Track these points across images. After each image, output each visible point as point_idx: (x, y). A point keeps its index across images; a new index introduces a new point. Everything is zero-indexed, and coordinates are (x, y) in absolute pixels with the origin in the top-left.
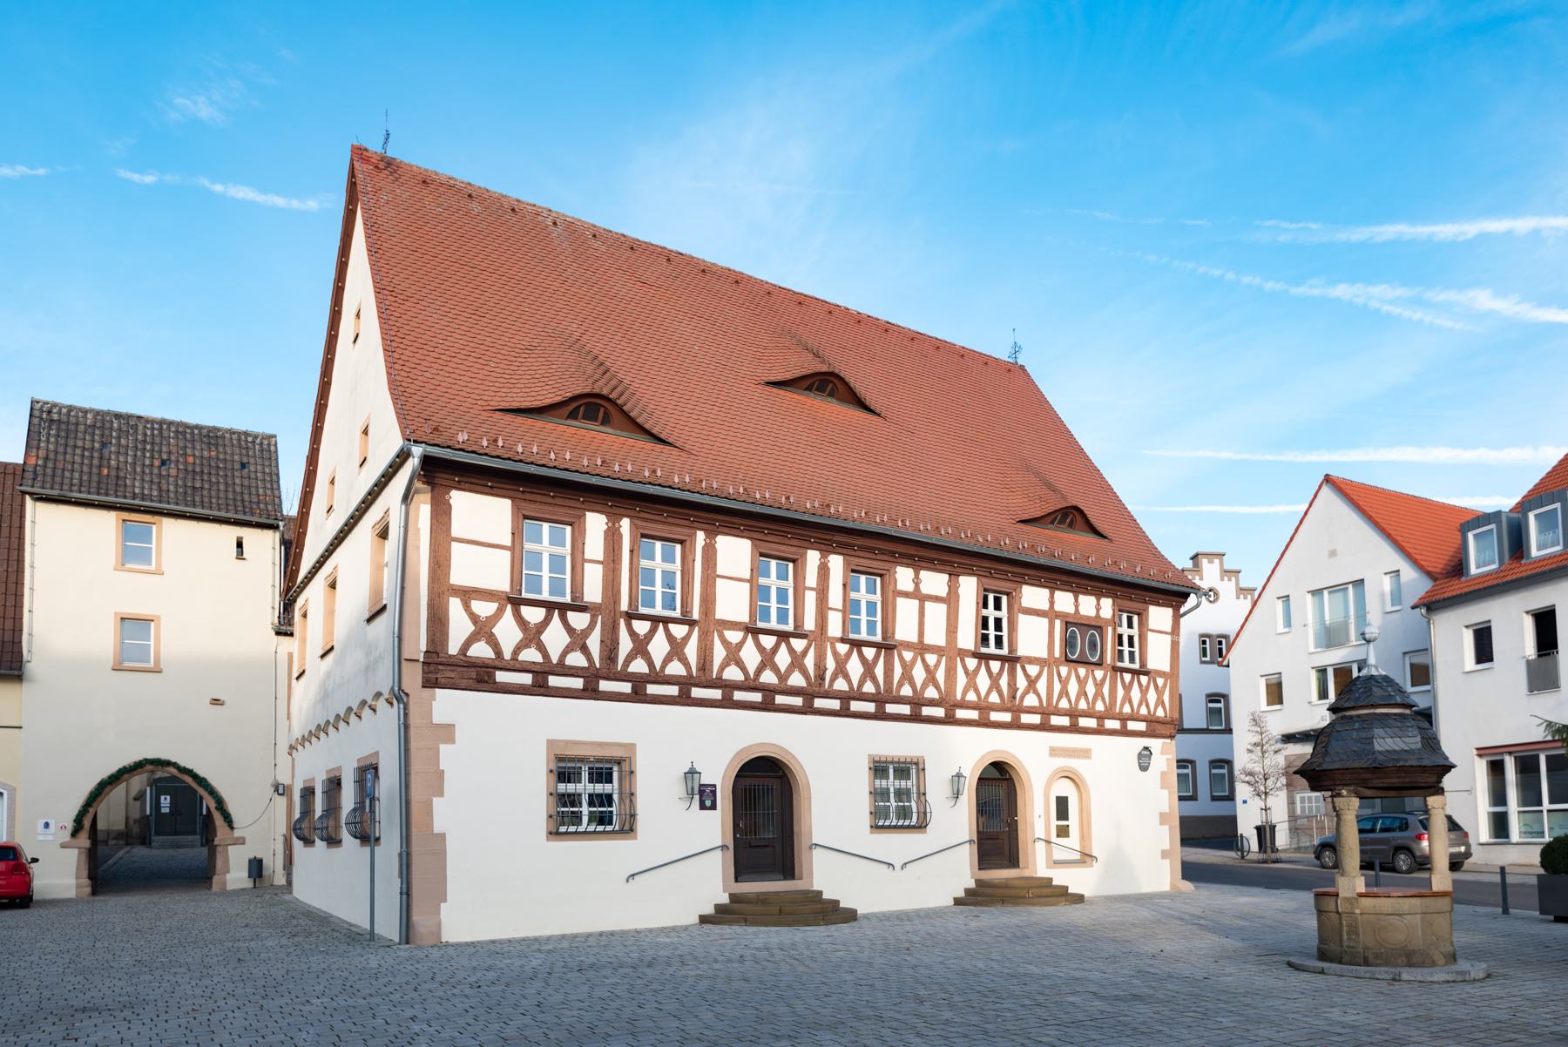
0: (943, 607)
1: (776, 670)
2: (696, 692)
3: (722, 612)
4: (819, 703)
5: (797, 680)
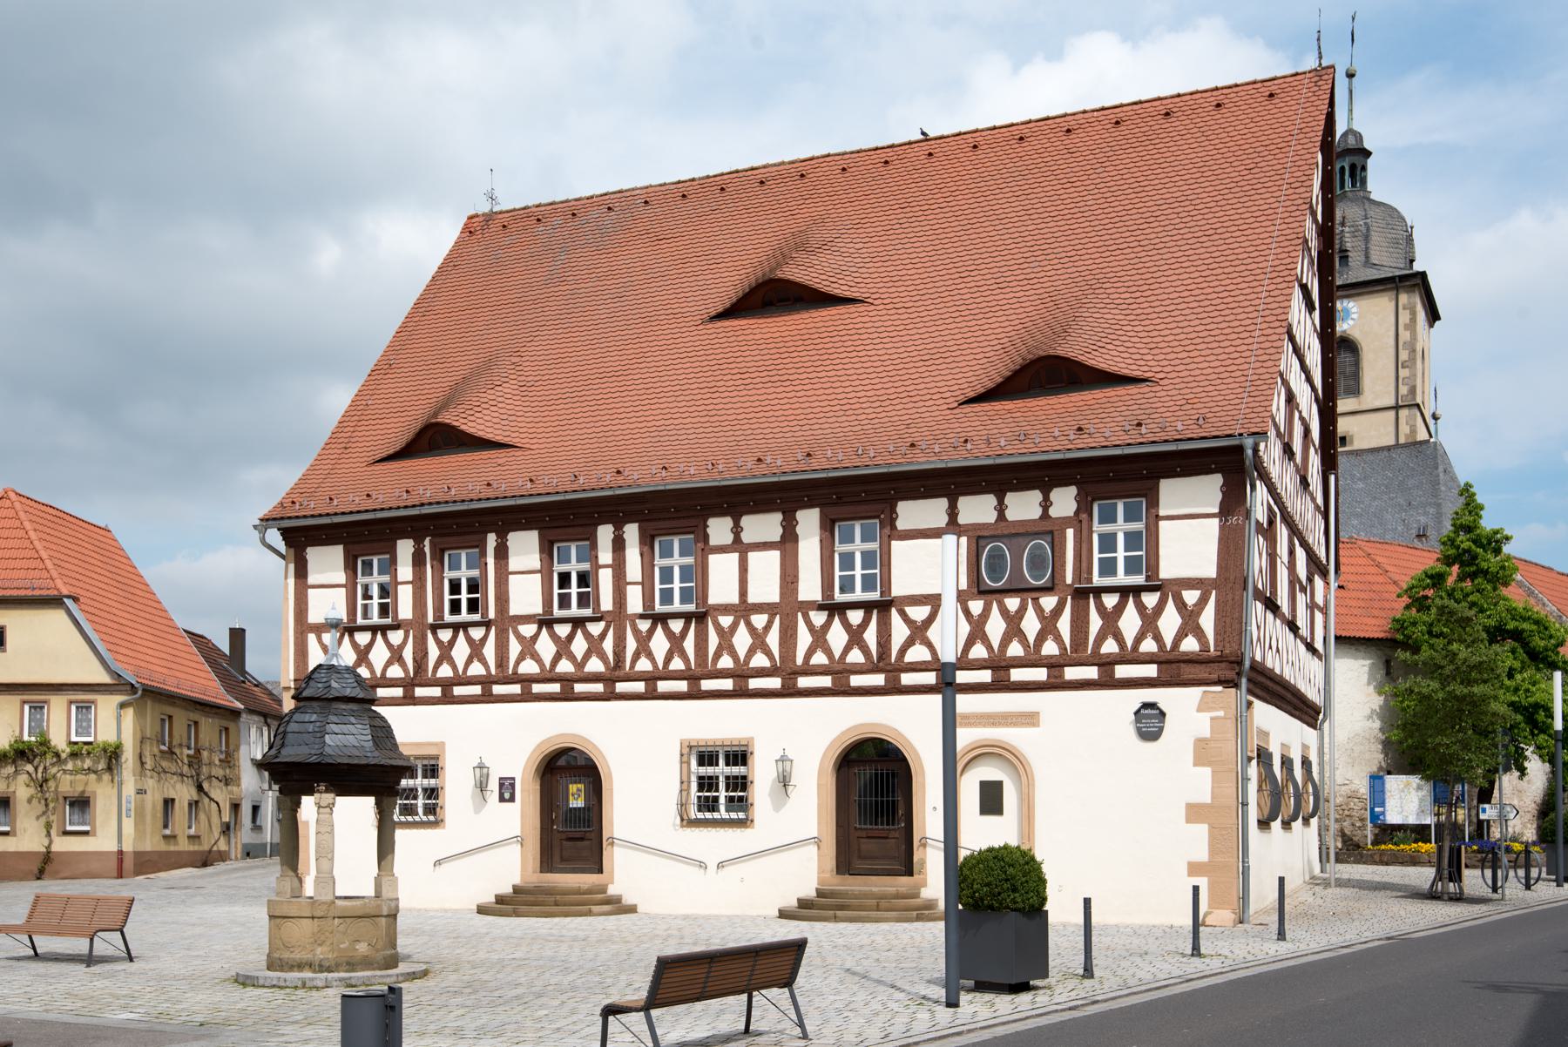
0: (775, 555)
1: (572, 658)
2: (498, 689)
3: (515, 609)
4: (621, 687)
5: (595, 665)
